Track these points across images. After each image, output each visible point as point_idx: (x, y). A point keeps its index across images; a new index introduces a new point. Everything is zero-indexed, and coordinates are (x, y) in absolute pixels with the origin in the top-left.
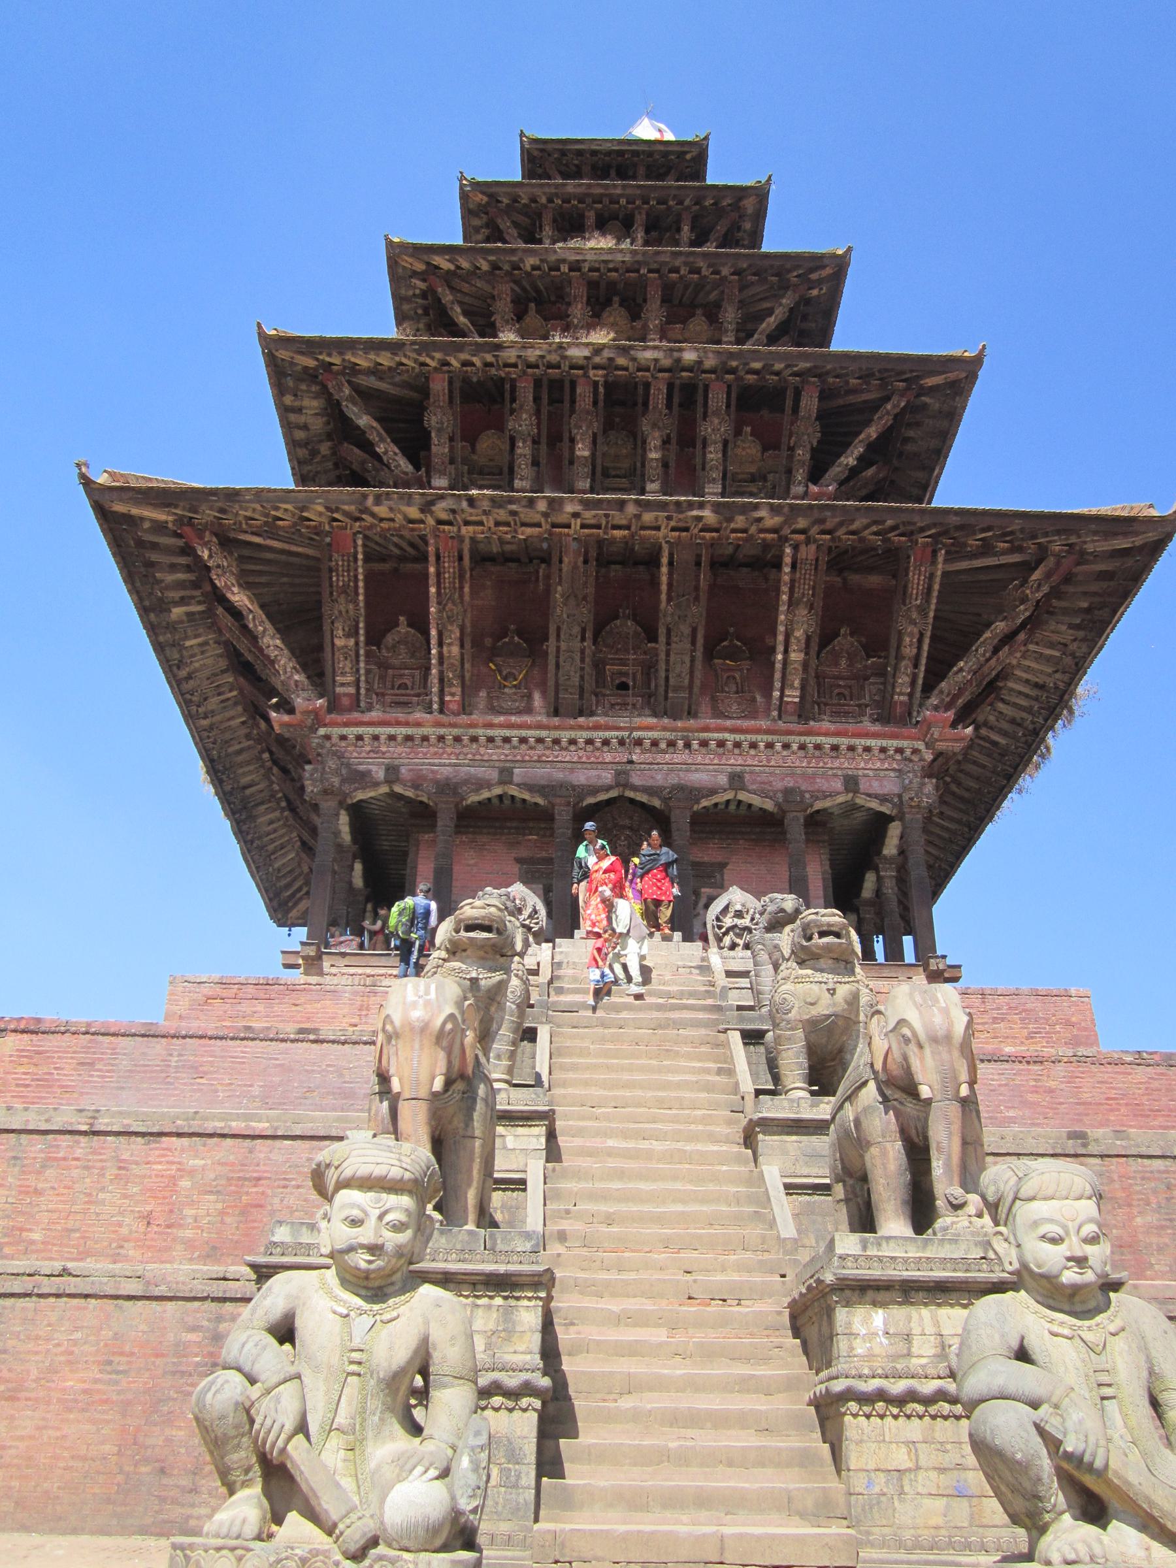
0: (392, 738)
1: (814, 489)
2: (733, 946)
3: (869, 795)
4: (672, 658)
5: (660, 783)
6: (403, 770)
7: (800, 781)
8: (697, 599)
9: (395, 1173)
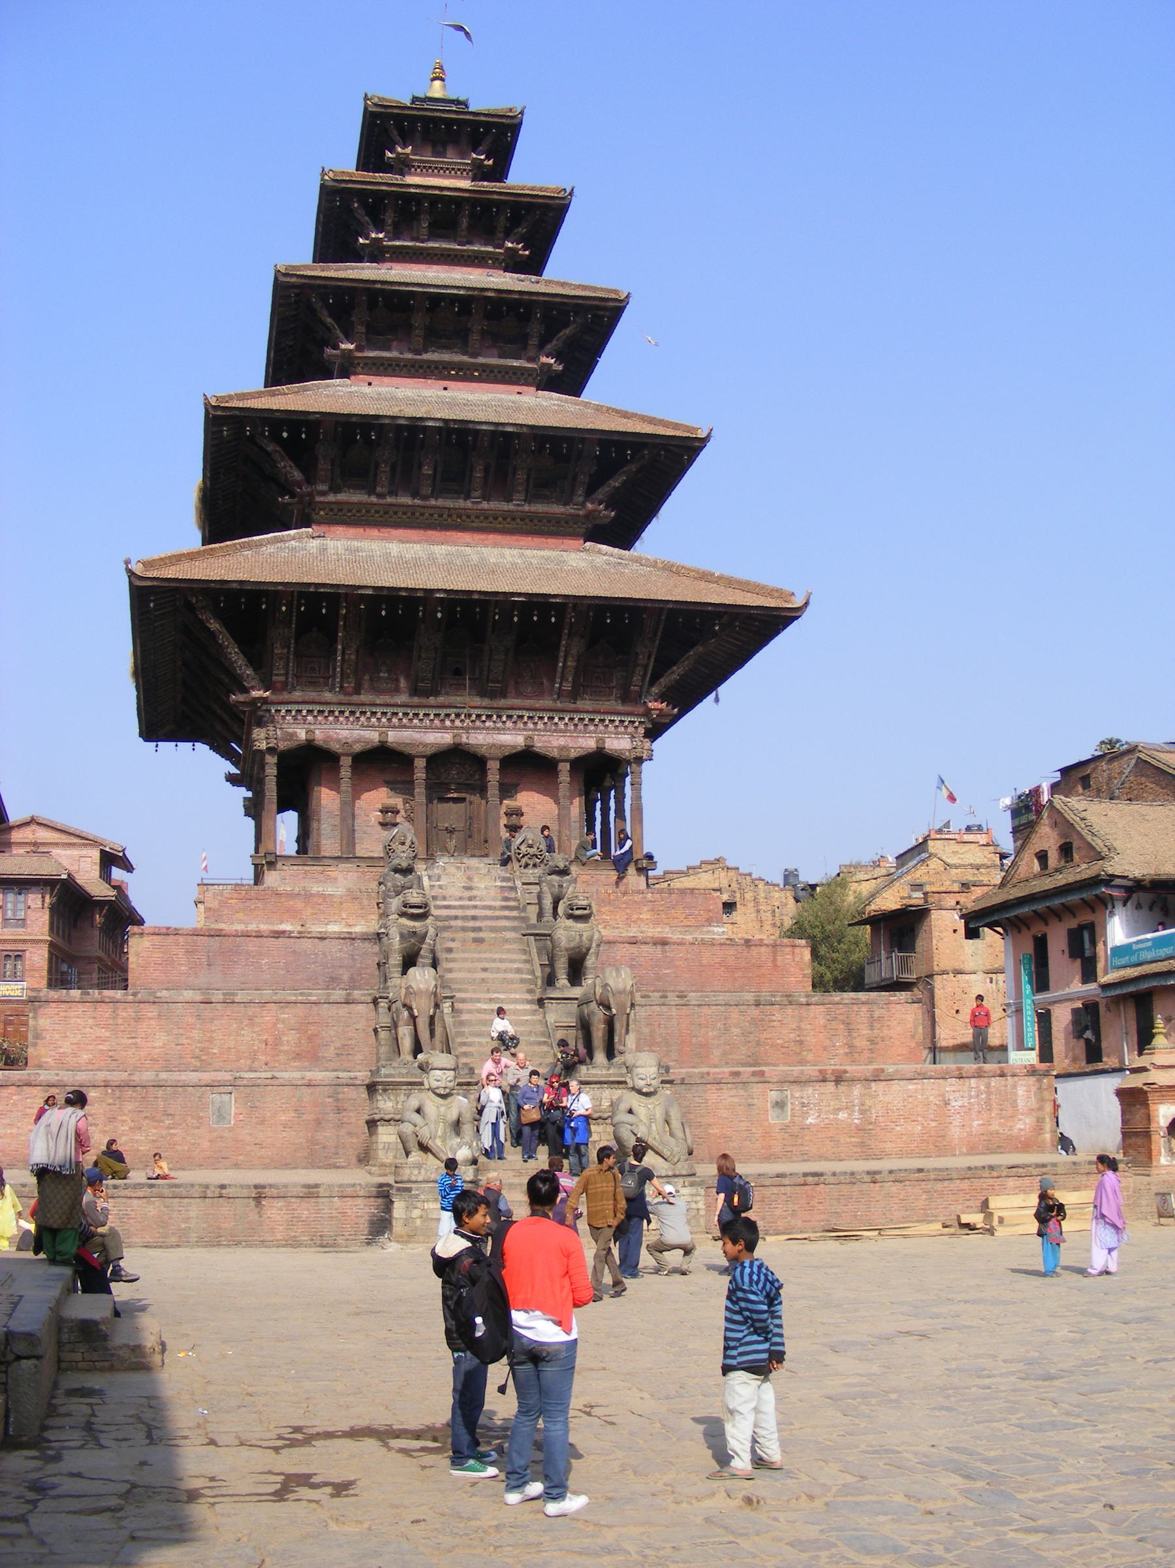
1: (589, 506)
2: (526, 866)
5: (481, 742)
6: (317, 732)
7: (568, 739)
9: (449, 1066)
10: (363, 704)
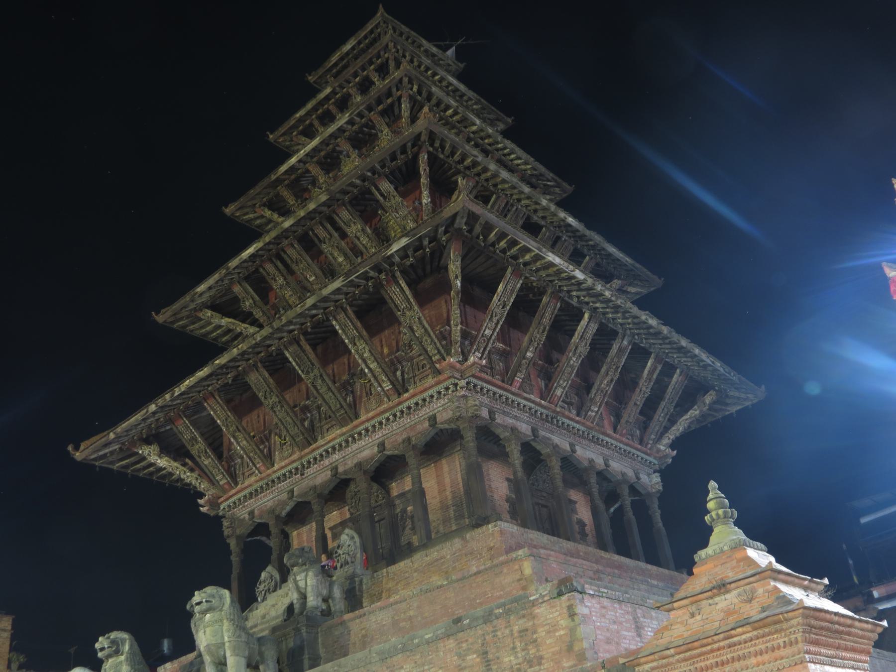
0: (245, 496)
3: (442, 423)
4: (325, 396)
6: (256, 511)
8: (313, 364)
10: (269, 475)
